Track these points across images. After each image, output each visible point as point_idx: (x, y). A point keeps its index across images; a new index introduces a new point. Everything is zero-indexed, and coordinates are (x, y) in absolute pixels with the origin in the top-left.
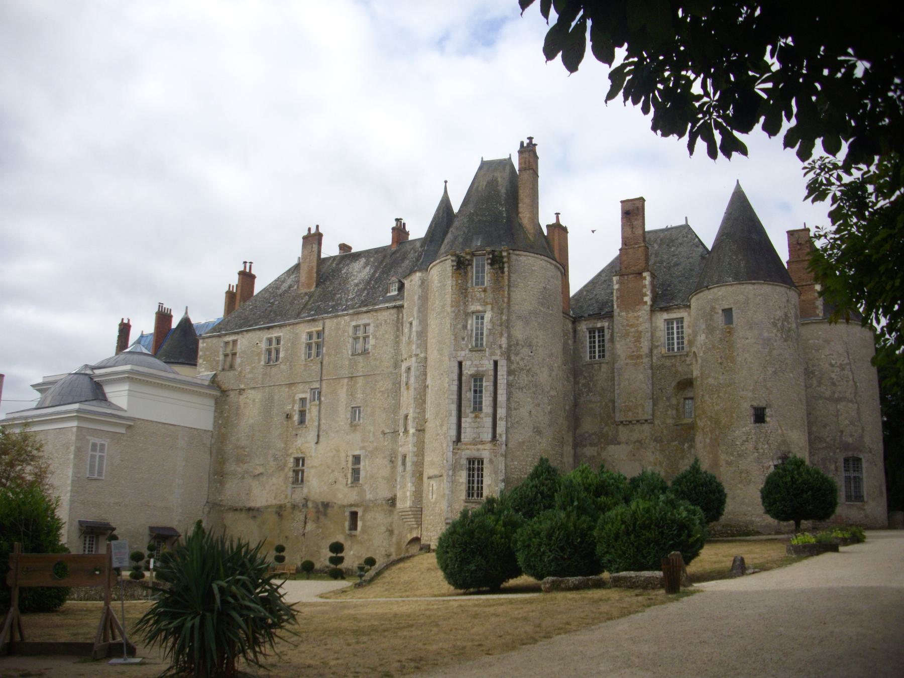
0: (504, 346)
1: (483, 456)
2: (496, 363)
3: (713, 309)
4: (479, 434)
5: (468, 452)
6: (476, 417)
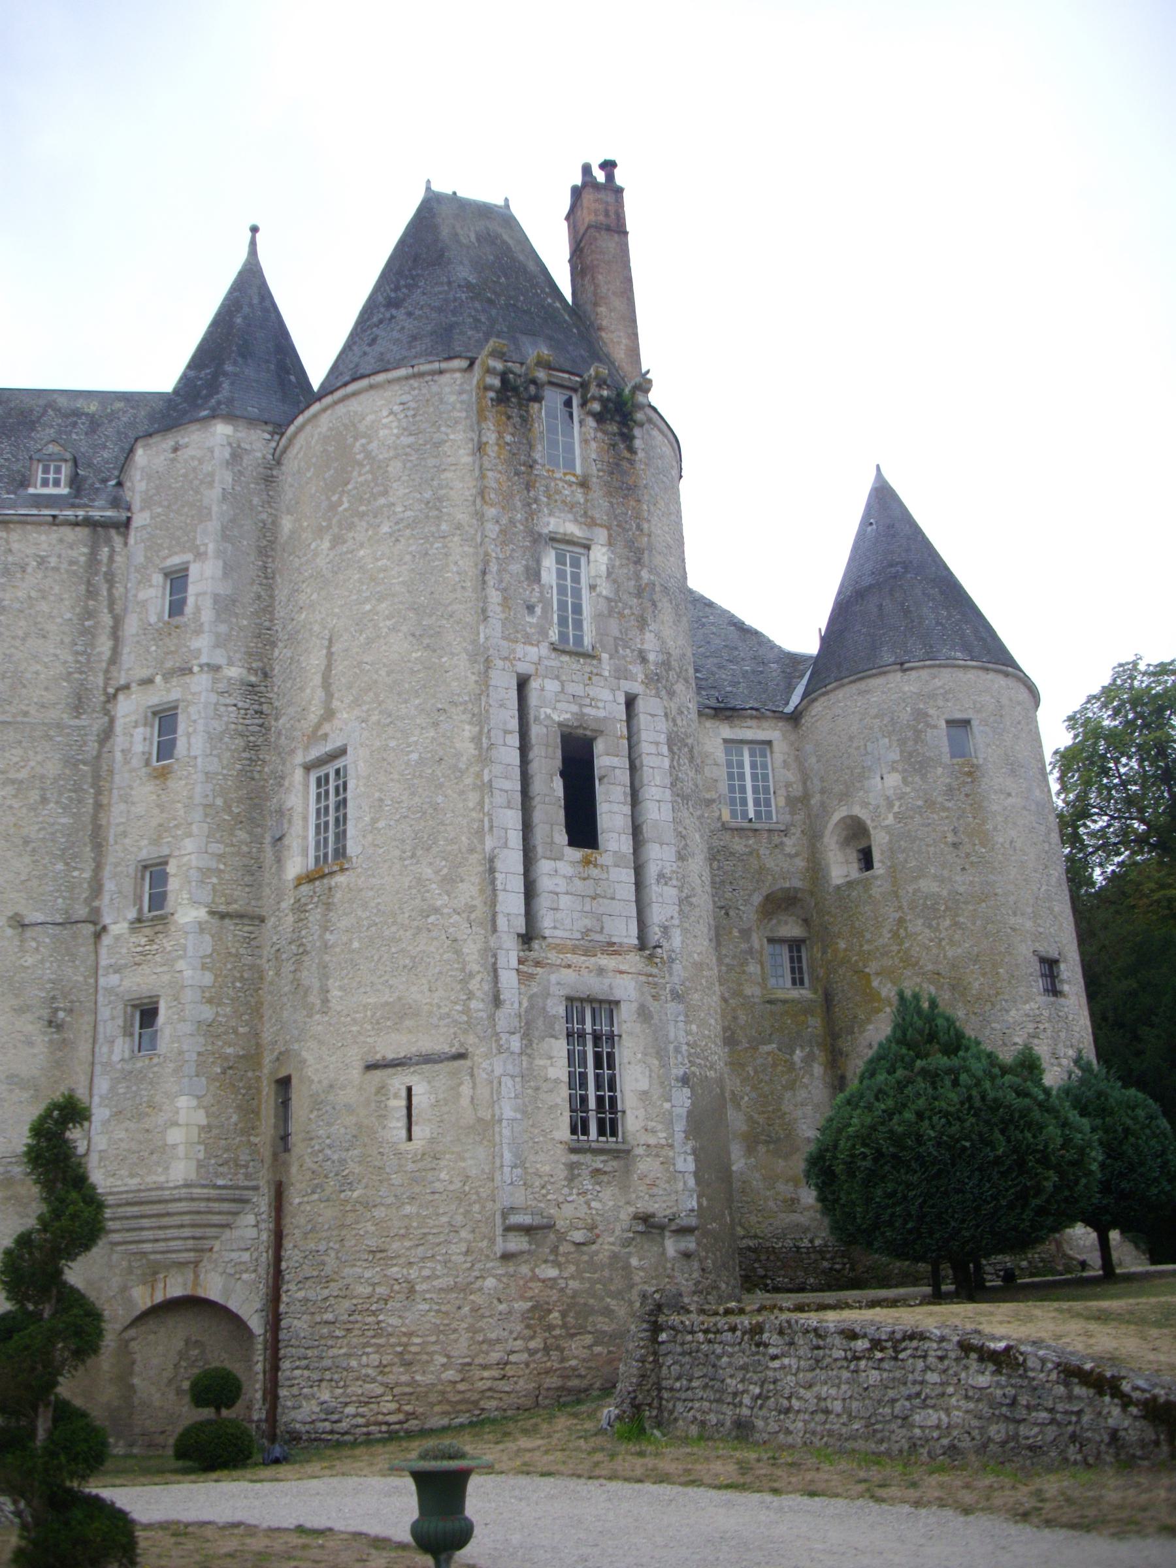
0: (652, 657)
1: (618, 994)
2: (630, 702)
3: (920, 715)
4: (599, 918)
5: (568, 975)
6: (587, 862)
